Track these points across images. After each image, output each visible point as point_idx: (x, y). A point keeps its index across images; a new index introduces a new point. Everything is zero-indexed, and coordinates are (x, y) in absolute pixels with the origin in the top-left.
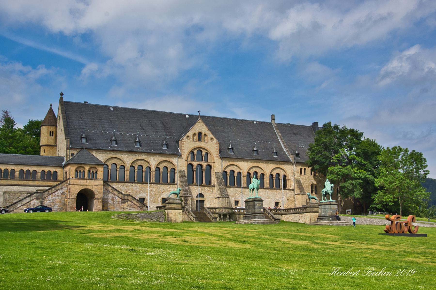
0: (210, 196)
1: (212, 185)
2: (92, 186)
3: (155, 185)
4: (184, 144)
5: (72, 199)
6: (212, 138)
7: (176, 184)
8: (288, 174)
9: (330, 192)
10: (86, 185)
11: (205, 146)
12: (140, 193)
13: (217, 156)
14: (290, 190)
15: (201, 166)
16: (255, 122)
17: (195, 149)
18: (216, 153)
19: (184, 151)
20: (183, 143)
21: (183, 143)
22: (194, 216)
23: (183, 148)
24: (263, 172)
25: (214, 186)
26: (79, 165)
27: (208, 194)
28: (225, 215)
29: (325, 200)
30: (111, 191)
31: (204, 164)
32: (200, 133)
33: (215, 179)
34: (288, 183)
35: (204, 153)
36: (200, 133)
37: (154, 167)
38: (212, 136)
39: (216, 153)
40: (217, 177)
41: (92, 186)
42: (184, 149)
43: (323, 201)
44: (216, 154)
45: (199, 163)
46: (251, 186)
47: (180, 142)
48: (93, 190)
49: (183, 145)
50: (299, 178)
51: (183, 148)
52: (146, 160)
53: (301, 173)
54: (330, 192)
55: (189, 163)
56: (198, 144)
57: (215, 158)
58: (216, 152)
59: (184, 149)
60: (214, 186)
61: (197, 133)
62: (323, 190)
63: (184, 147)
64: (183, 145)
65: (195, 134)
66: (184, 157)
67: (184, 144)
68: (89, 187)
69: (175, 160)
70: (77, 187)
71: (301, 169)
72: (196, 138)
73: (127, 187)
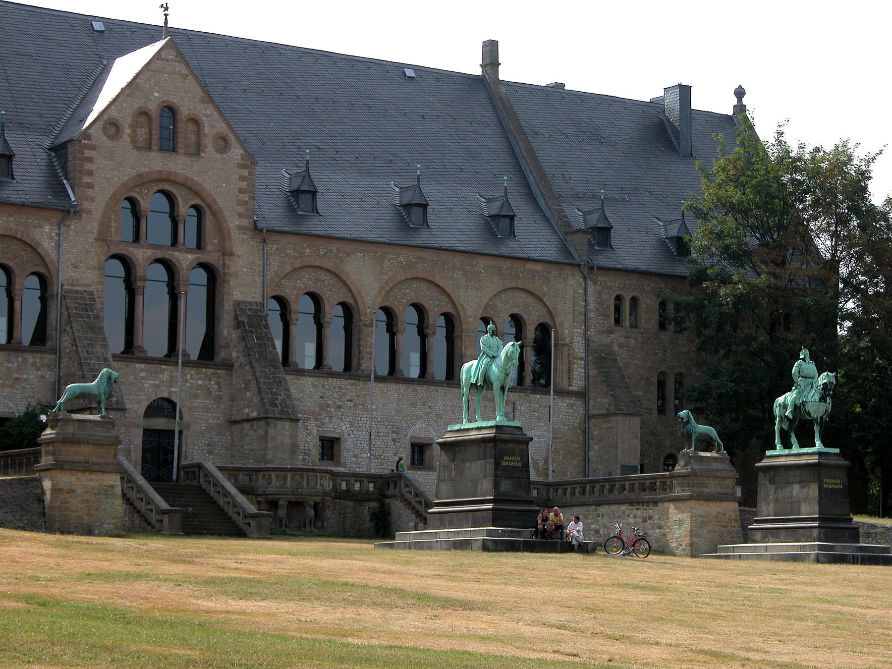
0: (207, 410)
1: (218, 359)
4: (90, 160)
6: (224, 139)
7: (54, 350)
8: (558, 320)
9: (817, 409)
11: (189, 174)
13: (246, 222)
14: (570, 394)
15: (169, 266)
16: (410, 73)
17: (142, 181)
18: (242, 209)
19: (89, 192)
20: (87, 153)
21: (87, 153)
22: (164, 505)
23: (87, 179)
24: (449, 309)
25: (228, 366)
27: (199, 401)
28: (296, 505)
29: (787, 445)
31: (185, 259)
32: (170, 111)
33: (235, 335)
34: (558, 365)
35: (184, 209)
38: (221, 127)
39: (242, 209)
40: (239, 325)
42: (90, 186)
43: (779, 450)
44: (241, 216)
45: (160, 255)
46: (470, 370)
47: (70, 149)
49: (88, 166)
50: (606, 340)
51: (87, 179)
53: (618, 321)
54: (817, 409)
57: (235, 235)
58: (240, 203)
59: (90, 186)
60: (228, 366)
61: (153, 107)
62: (780, 400)
63: (90, 173)
64: (88, 166)
65: (143, 113)
66: (91, 224)
67: (90, 160)
69: (44, 234)
71: (618, 298)
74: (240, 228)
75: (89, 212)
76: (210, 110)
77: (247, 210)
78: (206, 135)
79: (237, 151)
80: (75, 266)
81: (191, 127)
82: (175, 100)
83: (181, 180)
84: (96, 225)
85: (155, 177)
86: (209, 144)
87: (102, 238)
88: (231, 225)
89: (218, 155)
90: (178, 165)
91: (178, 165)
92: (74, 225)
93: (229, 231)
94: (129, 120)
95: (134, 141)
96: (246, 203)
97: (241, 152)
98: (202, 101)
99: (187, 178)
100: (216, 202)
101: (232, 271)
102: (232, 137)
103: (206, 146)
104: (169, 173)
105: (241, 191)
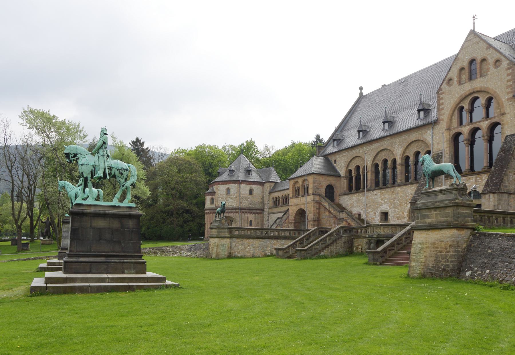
2: (304, 204)
3: (399, 189)
5: (291, 223)
6: (497, 61)
10: (300, 204)
12: (381, 205)
26: (295, 180)
30: (327, 207)
36: (472, 61)
37: (399, 157)
39: (509, 90)
41: (304, 204)
44: (508, 93)
48: (305, 209)
52: (389, 148)
55: (454, 131)
56: (468, 87)
57: (506, 104)
65: (462, 69)
66: (443, 125)
68: (302, 207)
69: (428, 135)
70: (294, 208)
72: (465, 76)
73: (367, 198)
74: (508, 99)
75: (443, 120)
76: (491, 50)
77: (511, 89)
78: (489, 64)
79: (505, 63)
80: (438, 144)
81: (484, 63)
82: (474, 55)
83: (478, 89)
84: (445, 124)
85: (467, 93)
86: (491, 67)
87: (448, 129)
88: (503, 100)
89: (496, 70)
90: (478, 84)
91: (478, 84)
92: (437, 127)
93: (503, 103)
94: (456, 75)
95: (460, 83)
96: (511, 86)
97: (508, 62)
98: (487, 49)
99: (481, 87)
100: (495, 92)
101: (505, 122)
102: (502, 58)
103: (489, 68)
104: (474, 89)
105: (508, 81)
